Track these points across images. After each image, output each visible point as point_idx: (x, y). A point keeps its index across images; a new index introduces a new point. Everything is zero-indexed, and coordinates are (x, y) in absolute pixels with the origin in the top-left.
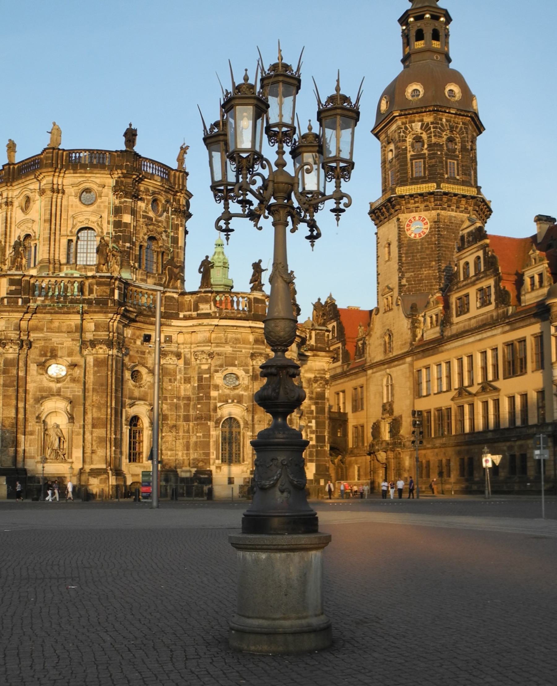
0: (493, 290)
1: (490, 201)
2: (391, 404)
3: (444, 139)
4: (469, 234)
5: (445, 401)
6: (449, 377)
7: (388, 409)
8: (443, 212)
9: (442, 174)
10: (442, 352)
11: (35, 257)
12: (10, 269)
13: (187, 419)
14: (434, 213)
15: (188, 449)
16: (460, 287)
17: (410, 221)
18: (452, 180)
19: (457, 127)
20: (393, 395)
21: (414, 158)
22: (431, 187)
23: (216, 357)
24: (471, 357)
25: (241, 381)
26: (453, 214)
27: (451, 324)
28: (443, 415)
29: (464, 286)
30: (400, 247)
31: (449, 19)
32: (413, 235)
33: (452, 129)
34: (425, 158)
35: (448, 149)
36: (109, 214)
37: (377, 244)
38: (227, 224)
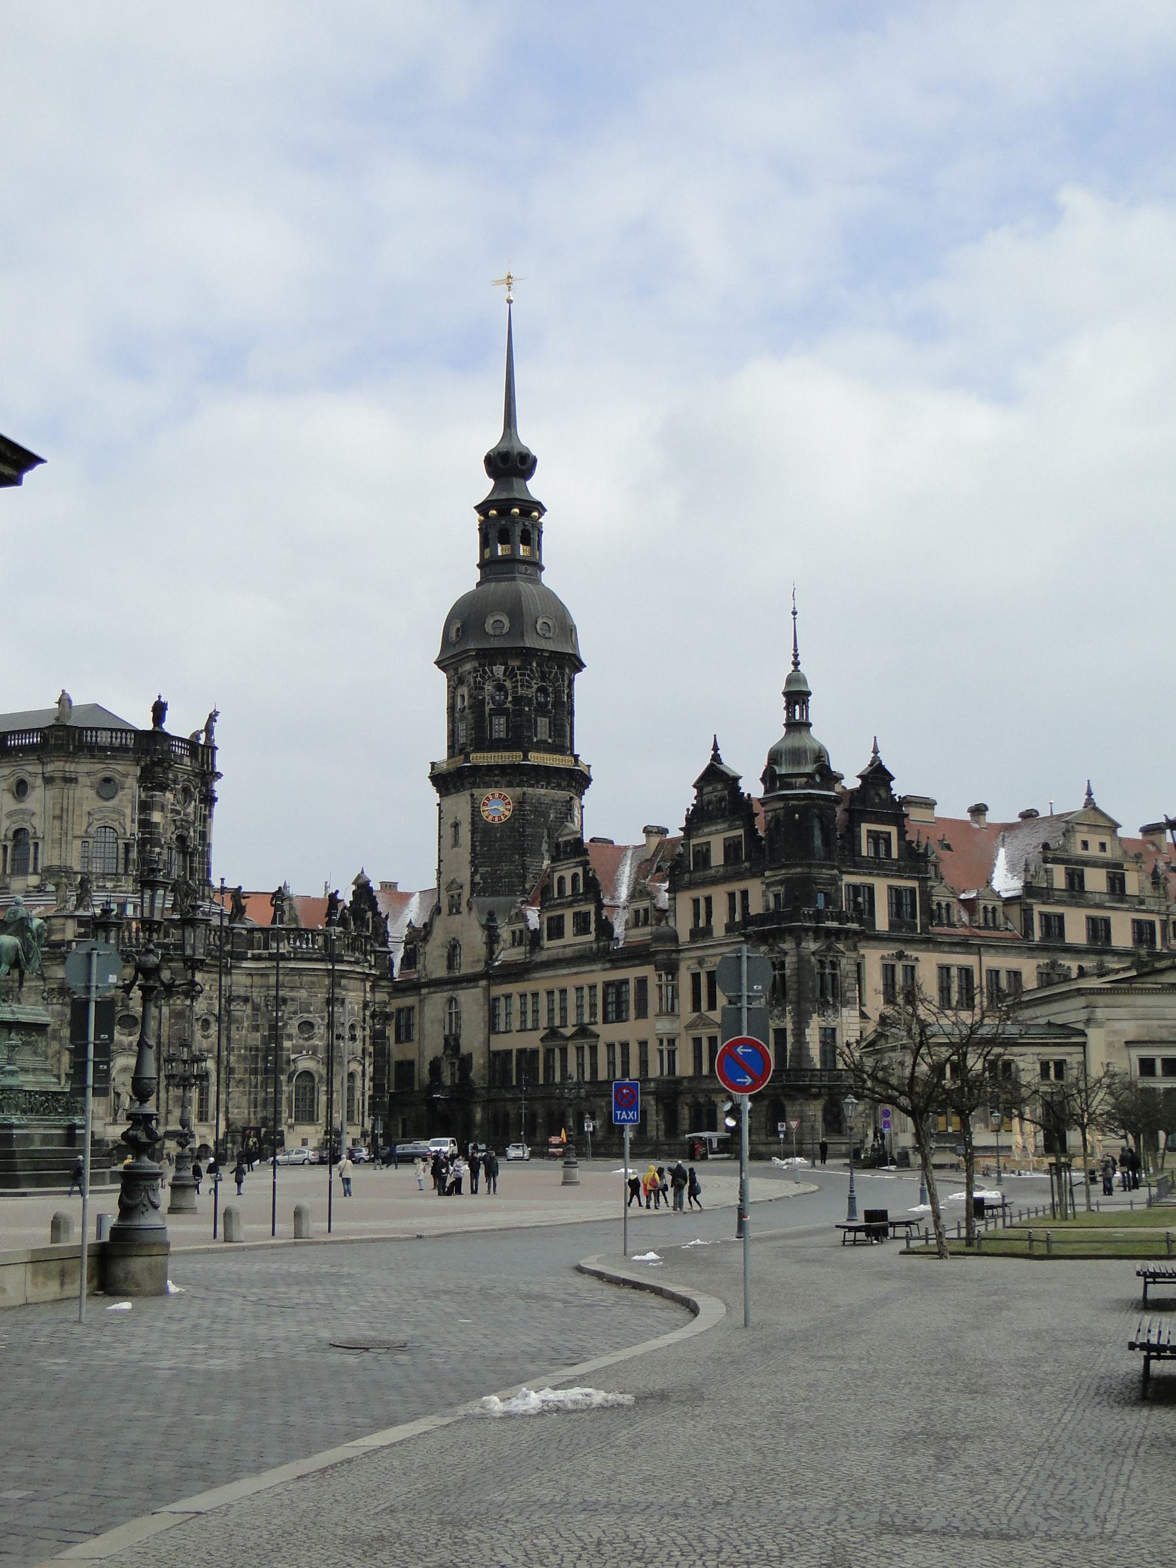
0: (593, 918)
1: (589, 766)
2: (457, 1038)
3: (534, 690)
4: (567, 843)
5: (533, 1041)
6: (536, 1012)
7: (452, 1043)
8: (530, 790)
9: (530, 738)
10: (529, 980)
11: (36, 859)
12: (76, 908)
13: (255, 1072)
14: (519, 790)
15: (256, 1107)
16: (553, 906)
18: (542, 747)
19: (551, 672)
20: (458, 1026)
21: (494, 713)
23: (289, 1002)
24: (563, 991)
25: (316, 1031)
26: (543, 791)
27: (542, 948)
28: (527, 1057)
29: (558, 905)
32: (490, 818)
33: (543, 677)
34: (508, 715)
35: (539, 703)
36: (133, 808)
37: (440, 818)
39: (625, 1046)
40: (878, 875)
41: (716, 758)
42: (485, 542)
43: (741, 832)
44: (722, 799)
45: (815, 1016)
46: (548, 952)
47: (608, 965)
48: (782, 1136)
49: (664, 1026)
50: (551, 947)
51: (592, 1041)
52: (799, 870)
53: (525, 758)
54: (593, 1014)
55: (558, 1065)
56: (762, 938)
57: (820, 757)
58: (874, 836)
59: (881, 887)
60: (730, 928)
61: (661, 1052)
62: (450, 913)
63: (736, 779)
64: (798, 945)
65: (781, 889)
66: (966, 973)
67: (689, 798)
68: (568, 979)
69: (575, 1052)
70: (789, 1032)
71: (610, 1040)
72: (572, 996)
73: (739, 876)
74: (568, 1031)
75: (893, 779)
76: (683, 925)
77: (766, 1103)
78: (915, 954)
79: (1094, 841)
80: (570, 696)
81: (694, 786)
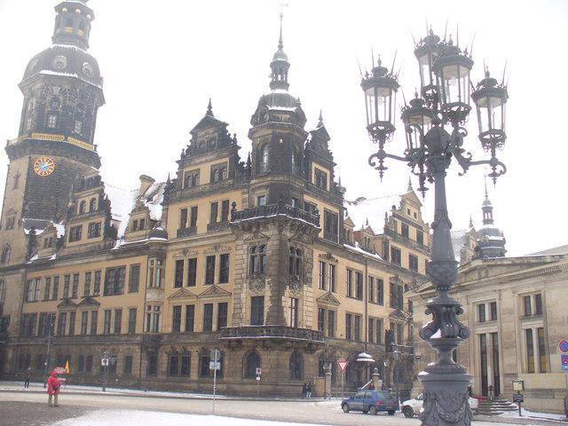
0: (103, 226)
5: (52, 307)
17: (39, 161)
18: (75, 136)
22: (60, 138)
24: (77, 275)
26: (73, 162)
27: (65, 247)
28: (47, 318)
30: (28, 180)
31: (93, 17)
33: (82, 98)
37: (8, 173)
38: (381, 162)
39: (119, 312)
40: (320, 199)
41: (210, 112)
42: (58, 25)
43: (227, 159)
44: (213, 139)
45: (288, 287)
46: (69, 250)
47: (111, 257)
48: (258, 378)
49: (152, 296)
50: (71, 246)
51: (94, 307)
52: (281, 178)
53: (66, 139)
54: (97, 290)
55: (68, 322)
56: (248, 228)
57: (297, 104)
58: (319, 173)
59: (321, 206)
60: (210, 227)
61: (149, 315)
62: (7, 228)
63: (225, 125)
64: (280, 231)
65: (266, 192)
66: (359, 275)
67: (185, 141)
68: (81, 267)
69: (81, 314)
70: (267, 299)
71: (108, 307)
72: (82, 279)
73: (223, 190)
74: (77, 301)
75: (329, 139)
76: (173, 227)
77: (242, 353)
78: (336, 257)
79: (413, 210)
80: (96, 113)
81: (191, 133)
